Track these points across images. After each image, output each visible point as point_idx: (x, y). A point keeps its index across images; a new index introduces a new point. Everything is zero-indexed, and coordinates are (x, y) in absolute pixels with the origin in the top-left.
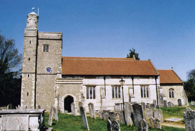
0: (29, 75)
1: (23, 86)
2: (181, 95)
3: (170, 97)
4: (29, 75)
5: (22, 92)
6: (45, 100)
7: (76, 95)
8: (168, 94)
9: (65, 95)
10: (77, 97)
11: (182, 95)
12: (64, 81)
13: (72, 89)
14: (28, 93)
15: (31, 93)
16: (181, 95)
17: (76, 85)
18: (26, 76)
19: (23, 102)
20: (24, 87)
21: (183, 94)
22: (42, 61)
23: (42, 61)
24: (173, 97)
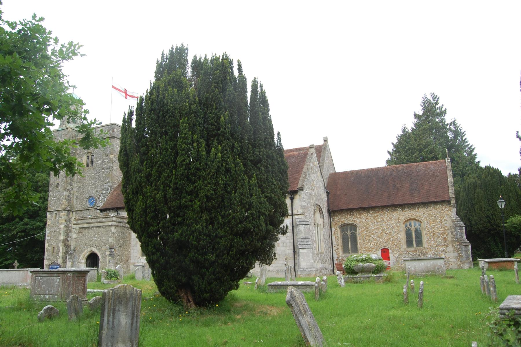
0: (56, 214)
1: (48, 236)
2: (445, 239)
3: (409, 243)
4: (56, 214)
5: (46, 246)
7: (103, 249)
8: (402, 236)
9: (84, 250)
10: (104, 253)
11: (450, 237)
12: (85, 223)
13: (95, 238)
14: (54, 248)
15: (58, 248)
16: (445, 239)
17: (101, 229)
18: (51, 217)
19: (46, 265)
20: (49, 238)
21: (452, 233)
22: (83, 185)
23: (83, 185)
24: (419, 243)
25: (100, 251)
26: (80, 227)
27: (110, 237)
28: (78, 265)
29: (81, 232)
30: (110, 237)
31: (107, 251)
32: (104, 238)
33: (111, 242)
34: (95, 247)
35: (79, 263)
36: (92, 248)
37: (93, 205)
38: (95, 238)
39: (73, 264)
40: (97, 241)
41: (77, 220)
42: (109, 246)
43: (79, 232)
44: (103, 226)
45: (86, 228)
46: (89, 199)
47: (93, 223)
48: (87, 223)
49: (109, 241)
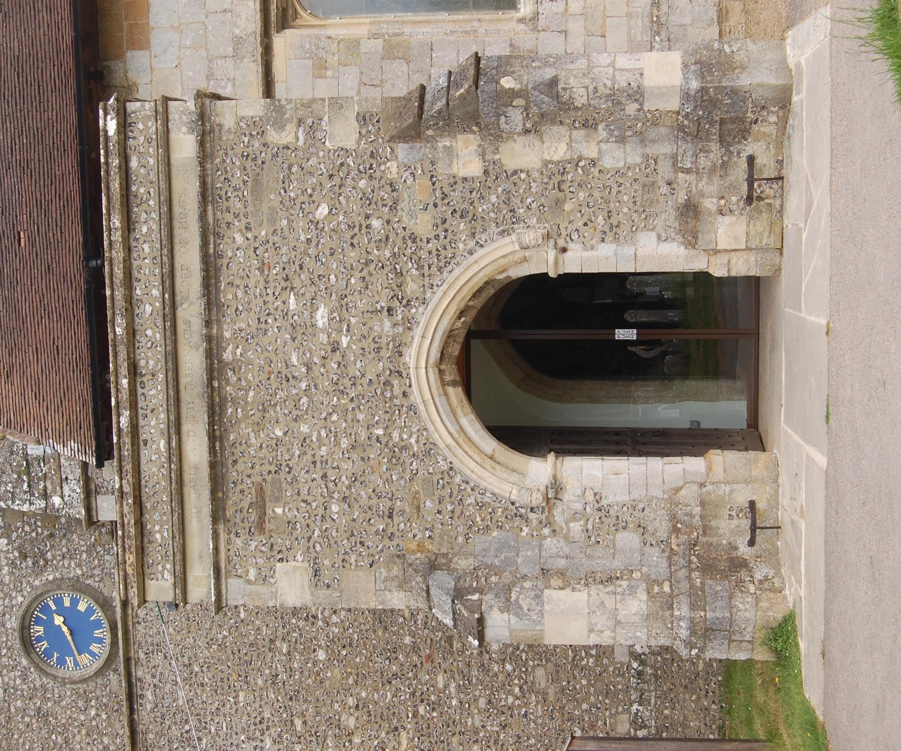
6: (528, 688)
7: (423, 225)
9: (430, 450)
12: (176, 454)
13: (321, 317)
25: (446, 263)
26: (207, 509)
27: (312, 130)
28: (576, 527)
29: (260, 505)
30: (312, 130)
31: (442, 170)
32: (323, 211)
33: (363, 119)
34: (409, 324)
35: (559, 517)
36: (410, 357)
37: (98, 614)
38: (321, 317)
39: (562, 574)
40: (343, 304)
41: (141, 552)
42: (402, 149)
43: (261, 525)
44: (203, 216)
45: (215, 437)
46: (48, 653)
47: (173, 359)
48: (176, 427)
49: (350, 144)
